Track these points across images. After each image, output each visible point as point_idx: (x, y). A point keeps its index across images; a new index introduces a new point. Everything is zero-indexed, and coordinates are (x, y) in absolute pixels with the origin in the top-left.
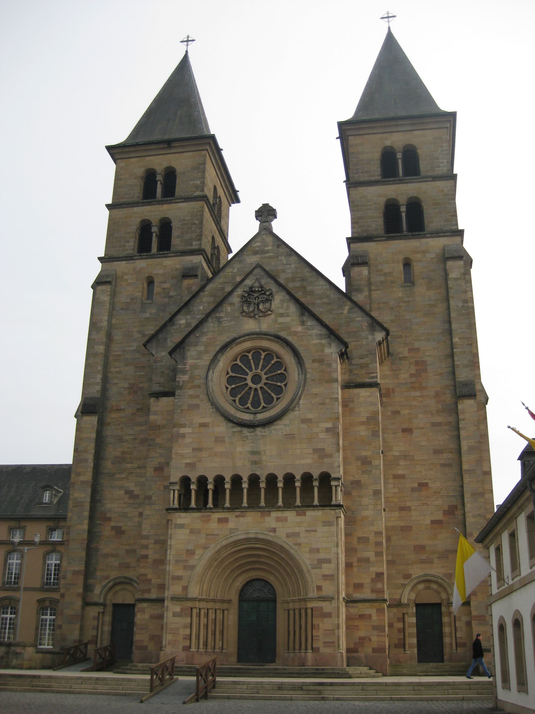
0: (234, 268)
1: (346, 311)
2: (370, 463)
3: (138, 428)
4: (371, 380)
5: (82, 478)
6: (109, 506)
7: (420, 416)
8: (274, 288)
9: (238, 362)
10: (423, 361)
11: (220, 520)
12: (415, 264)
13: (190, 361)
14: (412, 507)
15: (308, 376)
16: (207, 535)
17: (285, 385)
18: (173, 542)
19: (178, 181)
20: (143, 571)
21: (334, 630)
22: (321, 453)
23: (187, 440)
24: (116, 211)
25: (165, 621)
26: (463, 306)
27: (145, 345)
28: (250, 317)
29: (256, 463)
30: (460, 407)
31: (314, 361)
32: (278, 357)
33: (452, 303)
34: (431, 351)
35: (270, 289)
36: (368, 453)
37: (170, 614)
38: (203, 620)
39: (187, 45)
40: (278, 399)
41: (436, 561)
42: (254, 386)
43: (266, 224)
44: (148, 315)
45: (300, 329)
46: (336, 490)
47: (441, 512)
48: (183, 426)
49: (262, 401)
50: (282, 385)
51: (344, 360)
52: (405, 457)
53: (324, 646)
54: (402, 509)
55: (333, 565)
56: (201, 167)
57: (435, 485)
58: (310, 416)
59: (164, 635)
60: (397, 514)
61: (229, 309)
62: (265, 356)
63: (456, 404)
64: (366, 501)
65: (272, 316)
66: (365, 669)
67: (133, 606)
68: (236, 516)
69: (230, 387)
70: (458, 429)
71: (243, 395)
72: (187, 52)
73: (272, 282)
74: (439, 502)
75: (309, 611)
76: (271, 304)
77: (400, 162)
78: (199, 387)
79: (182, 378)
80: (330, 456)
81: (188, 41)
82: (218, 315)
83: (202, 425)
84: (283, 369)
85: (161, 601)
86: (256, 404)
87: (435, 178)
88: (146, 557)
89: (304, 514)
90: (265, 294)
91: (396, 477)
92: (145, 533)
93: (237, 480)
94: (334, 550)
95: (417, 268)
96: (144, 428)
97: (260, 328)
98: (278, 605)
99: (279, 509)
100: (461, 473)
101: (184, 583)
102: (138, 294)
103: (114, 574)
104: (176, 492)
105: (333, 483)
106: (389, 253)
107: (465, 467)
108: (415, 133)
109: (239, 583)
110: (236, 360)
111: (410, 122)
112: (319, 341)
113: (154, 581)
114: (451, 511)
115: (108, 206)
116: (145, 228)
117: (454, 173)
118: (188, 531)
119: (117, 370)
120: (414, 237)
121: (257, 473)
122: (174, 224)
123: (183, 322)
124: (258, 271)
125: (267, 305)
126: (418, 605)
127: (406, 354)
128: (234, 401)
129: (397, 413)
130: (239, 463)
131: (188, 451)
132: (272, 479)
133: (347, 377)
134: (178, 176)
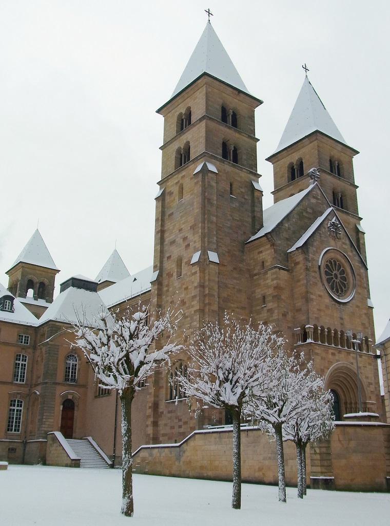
3: (235, 281)
83: (320, 296)
119: (221, 237)
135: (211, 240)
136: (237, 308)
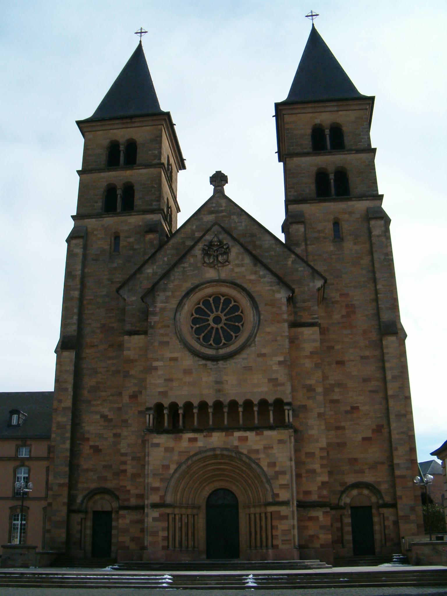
0: (193, 225)
1: (290, 263)
2: (314, 390)
3: (110, 362)
4: (313, 321)
5: (63, 405)
6: (87, 428)
7: (351, 351)
8: (231, 243)
9: (201, 305)
10: (351, 304)
11: (191, 440)
12: (343, 223)
13: (159, 305)
14: (346, 427)
15: (262, 317)
16: (179, 452)
17: (242, 325)
18: (151, 458)
19: (138, 150)
20: (122, 483)
21: (290, 530)
22: (274, 381)
23: (160, 372)
24: (84, 176)
25: (146, 525)
26: (385, 258)
27: (118, 291)
28: (211, 267)
29: (219, 391)
30: (384, 343)
31: (266, 305)
32: (235, 302)
33: (376, 256)
34: (359, 296)
35: (227, 244)
36: (312, 382)
37: (150, 520)
38: (178, 524)
39: (141, 36)
40: (236, 337)
41: (367, 471)
42: (215, 326)
43: (219, 188)
44: (115, 265)
45: (253, 277)
46: (288, 415)
47: (370, 431)
48: (157, 360)
49: (223, 339)
50: (240, 325)
51: (290, 304)
52: (339, 385)
53: (283, 544)
54: (338, 428)
55: (288, 477)
56: (158, 139)
57: (364, 409)
58: (264, 351)
59: (146, 537)
60: (333, 432)
61: (192, 260)
62: (224, 300)
63: (381, 341)
64: (311, 422)
65: (230, 267)
66: (317, 562)
67: (109, 513)
68: (204, 436)
69: (195, 327)
70: (383, 361)
71: (206, 333)
72: (140, 42)
73: (229, 237)
74: (368, 422)
75: (269, 515)
76: (228, 257)
77: (328, 136)
78: (168, 326)
79: (153, 319)
80: (283, 384)
81: (141, 33)
82: (182, 265)
84: (240, 311)
85: (141, 508)
86: (217, 341)
87: (358, 151)
88: (125, 471)
89: (263, 434)
90: (222, 247)
91: (332, 401)
92: (123, 451)
93: (203, 405)
94: (288, 463)
95: (345, 227)
96: (115, 361)
97: (219, 276)
98: (240, 510)
99: (239, 429)
100: (386, 398)
101: (162, 493)
102: (107, 247)
103: (93, 486)
104: (151, 416)
105: (286, 407)
106: (321, 212)
107: (390, 393)
108: (340, 113)
109: (206, 492)
110: (199, 304)
111: (336, 104)
112: (270, 288)
113: (134, 491)
114: (378, 429)
115: (78, 172)
116: (111, 190)
117: (373, 147)
118: (162, 449)
120: (341, 200)
121: (221, 400)
122: (137, 187)
123: (150, 271)
124: (216, 228)
125: (225, 256)
126: (352, 508)
127: (338, 298)
128: (199, 339)
129: (332, 348)
130: (205, 392)
131: (161, 381)
132: (233, 404)
133: (292, 318)
134: (138, 147)
135: (69, 321)
136: (112, 395)
